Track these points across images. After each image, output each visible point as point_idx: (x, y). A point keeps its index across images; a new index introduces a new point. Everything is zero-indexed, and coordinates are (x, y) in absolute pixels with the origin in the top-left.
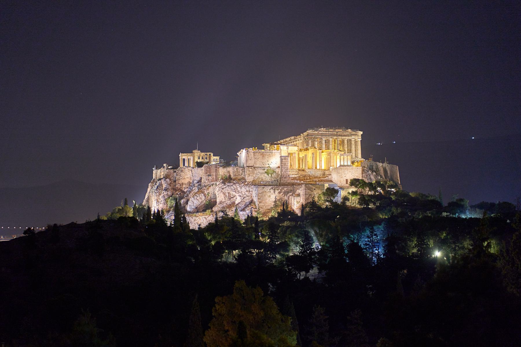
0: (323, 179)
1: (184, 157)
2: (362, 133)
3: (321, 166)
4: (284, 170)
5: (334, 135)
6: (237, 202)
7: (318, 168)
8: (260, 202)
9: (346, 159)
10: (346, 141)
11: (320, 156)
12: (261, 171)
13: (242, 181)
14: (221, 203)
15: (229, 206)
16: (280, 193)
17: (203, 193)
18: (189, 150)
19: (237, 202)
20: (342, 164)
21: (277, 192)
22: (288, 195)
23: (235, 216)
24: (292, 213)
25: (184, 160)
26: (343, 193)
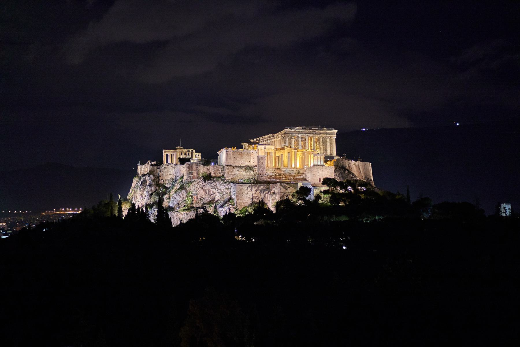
0: (298, 177)
1: (167, 153)
2: (336, 131)
3: (296, 165)
4: (261, 169)
5: (309, 133)
6: (216, 199)
7: (293, 166)
8: (238, 200)
9: (319, 159)
10: (321, 139)
11: (295, 155)
12: (240, 170)
13: (221, 178)
14: (201, 199)
15: (210, 203)
16: (256, 191)
17: (185, 189)
18: (173, 147)
19: (216, 199)
20: (316, 163)
21: (254, 189)
22: (264, 193)
23: (215, 212)
24: (269, 211)
25: (167, 156)
26: (315, 192)
